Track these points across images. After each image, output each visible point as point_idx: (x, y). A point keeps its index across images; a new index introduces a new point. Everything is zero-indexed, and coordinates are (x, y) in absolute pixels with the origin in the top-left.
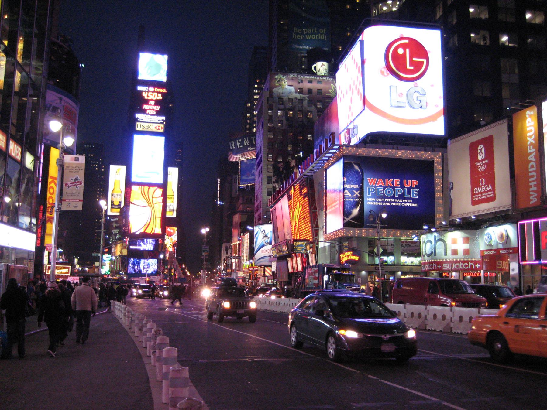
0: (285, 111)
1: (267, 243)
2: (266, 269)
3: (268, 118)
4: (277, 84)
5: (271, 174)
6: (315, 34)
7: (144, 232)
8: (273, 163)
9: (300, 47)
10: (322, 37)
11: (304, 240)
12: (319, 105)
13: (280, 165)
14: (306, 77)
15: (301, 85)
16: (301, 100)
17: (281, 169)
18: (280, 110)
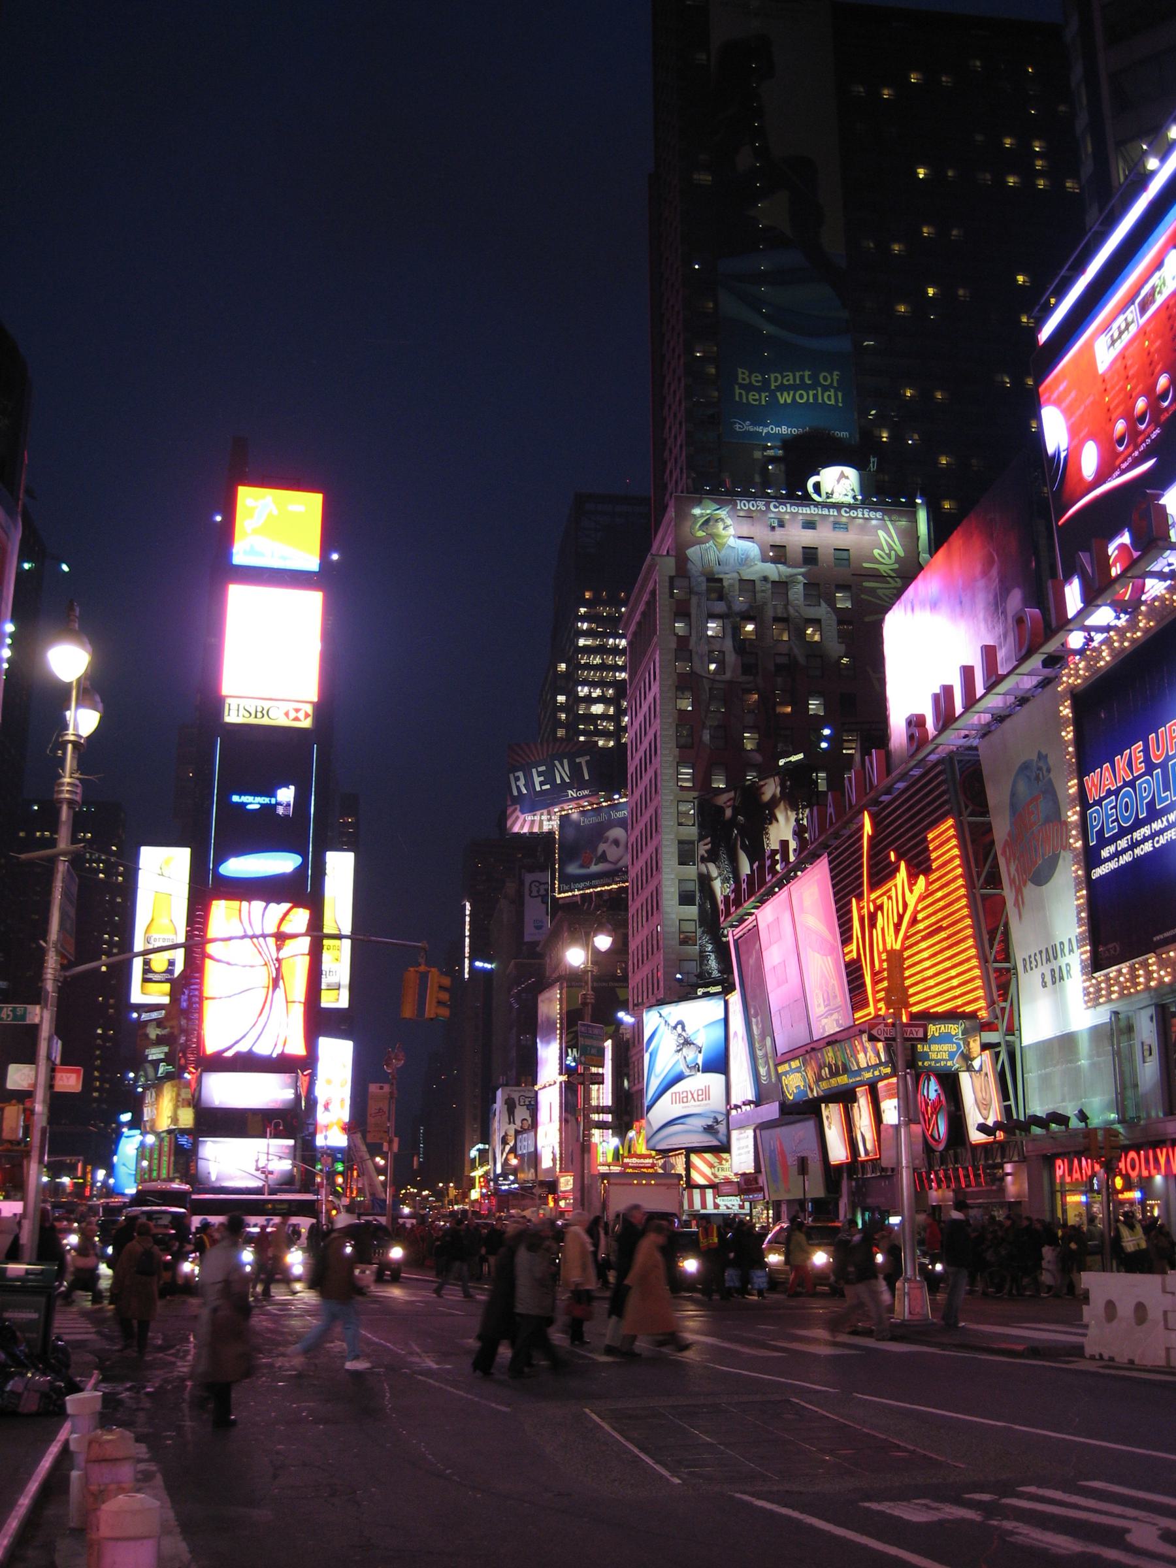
0: (732, 620)
1: (695, 1068)
2: (694, 1158)
3: (674, 646)
4: (701, 534)
5: (692, 832)
6: (807, 388)
7: (250, 1050)
8: (695, 794)
9: (760, 429)
10: (830, 398)
11: (951, 1016)
12: (843, 600)
13: (722, 800)
14: (794, 509)
15: (778, 537)
16: (781, 586)
17: (729, 813)
18: (712, 616)
